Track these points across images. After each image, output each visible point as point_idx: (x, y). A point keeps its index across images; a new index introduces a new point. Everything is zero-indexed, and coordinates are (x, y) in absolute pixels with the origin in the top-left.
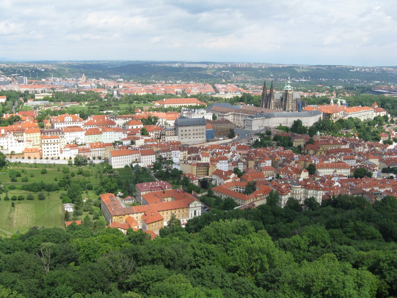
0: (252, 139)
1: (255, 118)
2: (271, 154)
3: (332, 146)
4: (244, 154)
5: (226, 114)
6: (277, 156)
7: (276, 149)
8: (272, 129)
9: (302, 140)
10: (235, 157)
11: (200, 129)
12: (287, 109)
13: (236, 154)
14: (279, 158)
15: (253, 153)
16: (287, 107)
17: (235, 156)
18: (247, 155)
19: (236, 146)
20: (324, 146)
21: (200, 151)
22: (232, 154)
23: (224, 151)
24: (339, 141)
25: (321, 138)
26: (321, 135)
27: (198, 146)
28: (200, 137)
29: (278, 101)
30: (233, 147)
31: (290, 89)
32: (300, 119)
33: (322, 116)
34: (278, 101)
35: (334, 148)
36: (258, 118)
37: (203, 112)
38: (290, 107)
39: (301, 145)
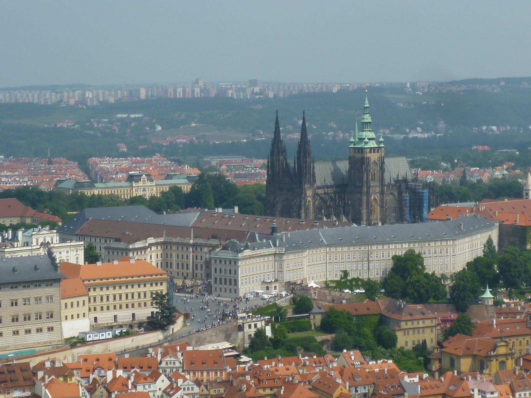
0: (240, 328)
1: (247, 253)
2: (315, 378)
4: (210, 384)
5: (139, 245)
6: (339, 381)
7: (331, 362)
8: (312, 292)
9: (428, 323)
10: (179, 393)
11: (38, 300)
12: (365, 218)
13: (180, 382)
14: (346, 391)
15: (248, 378)
16: (364, 211)
17: (178, 389)
18: (227, 383)
19: (179, 354)
20: (513, 339)
21: (43, 379)
22: (167, 383)
23: (135, 372)
25: (499, 314)
26: (497, 303)
27: (34, 362)
28: (39, 330)
29: (330, 190)
30: (168, 359)
31: (373, 144)
32: (417, 248)
33: (494, 234)
37: (48, 239)
38: (378, 209)
39: (424, 342)
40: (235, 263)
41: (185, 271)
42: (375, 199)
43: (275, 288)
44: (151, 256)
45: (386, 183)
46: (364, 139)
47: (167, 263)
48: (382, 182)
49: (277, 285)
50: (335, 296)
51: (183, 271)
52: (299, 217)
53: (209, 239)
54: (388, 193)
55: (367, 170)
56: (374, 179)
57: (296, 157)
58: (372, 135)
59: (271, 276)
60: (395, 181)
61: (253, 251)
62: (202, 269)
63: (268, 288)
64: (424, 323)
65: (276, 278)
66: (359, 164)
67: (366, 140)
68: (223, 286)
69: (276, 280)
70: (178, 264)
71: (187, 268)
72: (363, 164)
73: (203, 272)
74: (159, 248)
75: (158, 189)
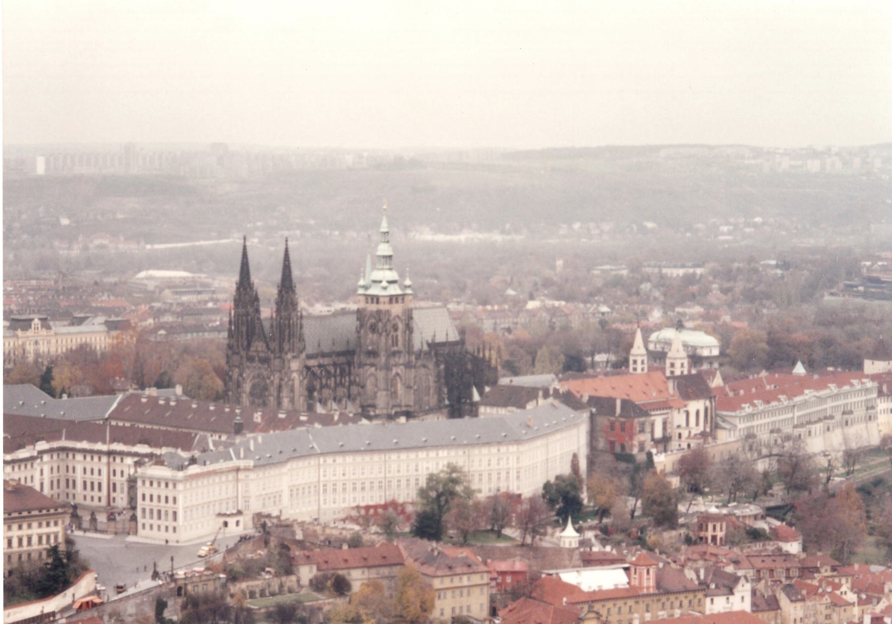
1: (194, 469)
3: (655, 606)
9: (476, 579)
20: (609, 604)
24: (690, 574)
29: (325, 361)
31: (395, 290)
34: (325, 361)
35: (662, 614)
36: (210, 467)
40: (175, 486)
41: (96, 493)
43: (238, 523)
44: (42, 471)
47: (68, 481)
48: (409, 347)
49: (240, 518)
50: (333, 535)
51: (93, 494)
52: (279, 404)
53: (134, 444)
55: (386, 331)
57: (274, 310)
58: (393, 275)
59: (231, 505)
60: (429, 345)
61: (203, 467)
62: (122, 492)
63: (226, 524)
64: (469, 579)
65: (240, 508)
67: (384, 284)
68: (155, 522)
69: (240, 513)
70: (85, 483)
71: (100, 489)
73: (125, 496)
74: (55, 456)
75: (59, 342)
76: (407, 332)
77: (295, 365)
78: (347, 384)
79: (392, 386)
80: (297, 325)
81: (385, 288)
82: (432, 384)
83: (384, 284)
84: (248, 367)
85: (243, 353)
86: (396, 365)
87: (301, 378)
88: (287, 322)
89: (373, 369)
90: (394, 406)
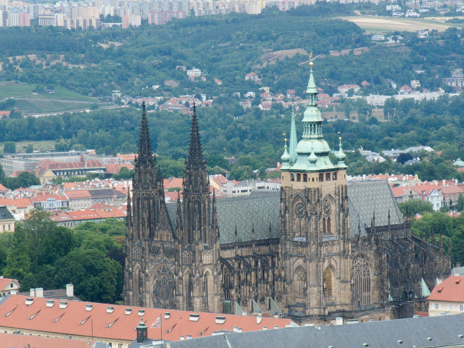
12: (313, 302)
29: (244, 252)
31: (325, 164)
42: (330, 266)
45: (352, 234)
46: (309, 154)
48: (344, 233)
54: (356, 254)
55: (316, 214)
56: (327, 229)
60: (368, 230)
66: (300, 201)
67: (313, 157)
72: (308, 201)
76: (341, 214)
77: (207, 258)
78: (270, 279)
79: (324, 280)
80: (209, 209)
81: (314, 162)
82: (372, 277)
83: (313, 157)
84: (152, 261)
85: (145, 244)
86: (330, 256)
87: (215, 273)
88: (197, 206)
89: (300, 261)
90: (327, 305)
